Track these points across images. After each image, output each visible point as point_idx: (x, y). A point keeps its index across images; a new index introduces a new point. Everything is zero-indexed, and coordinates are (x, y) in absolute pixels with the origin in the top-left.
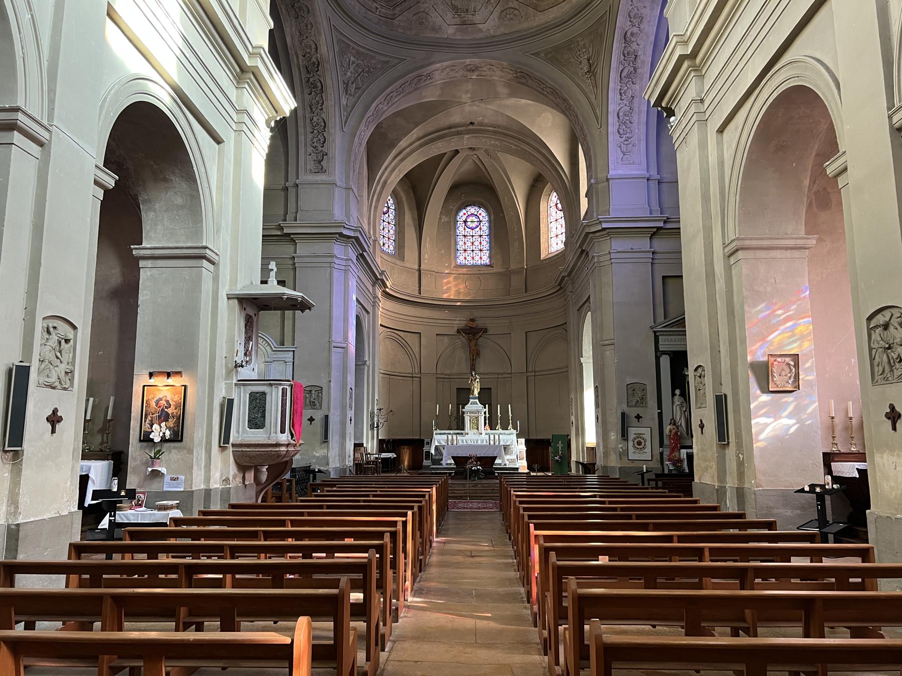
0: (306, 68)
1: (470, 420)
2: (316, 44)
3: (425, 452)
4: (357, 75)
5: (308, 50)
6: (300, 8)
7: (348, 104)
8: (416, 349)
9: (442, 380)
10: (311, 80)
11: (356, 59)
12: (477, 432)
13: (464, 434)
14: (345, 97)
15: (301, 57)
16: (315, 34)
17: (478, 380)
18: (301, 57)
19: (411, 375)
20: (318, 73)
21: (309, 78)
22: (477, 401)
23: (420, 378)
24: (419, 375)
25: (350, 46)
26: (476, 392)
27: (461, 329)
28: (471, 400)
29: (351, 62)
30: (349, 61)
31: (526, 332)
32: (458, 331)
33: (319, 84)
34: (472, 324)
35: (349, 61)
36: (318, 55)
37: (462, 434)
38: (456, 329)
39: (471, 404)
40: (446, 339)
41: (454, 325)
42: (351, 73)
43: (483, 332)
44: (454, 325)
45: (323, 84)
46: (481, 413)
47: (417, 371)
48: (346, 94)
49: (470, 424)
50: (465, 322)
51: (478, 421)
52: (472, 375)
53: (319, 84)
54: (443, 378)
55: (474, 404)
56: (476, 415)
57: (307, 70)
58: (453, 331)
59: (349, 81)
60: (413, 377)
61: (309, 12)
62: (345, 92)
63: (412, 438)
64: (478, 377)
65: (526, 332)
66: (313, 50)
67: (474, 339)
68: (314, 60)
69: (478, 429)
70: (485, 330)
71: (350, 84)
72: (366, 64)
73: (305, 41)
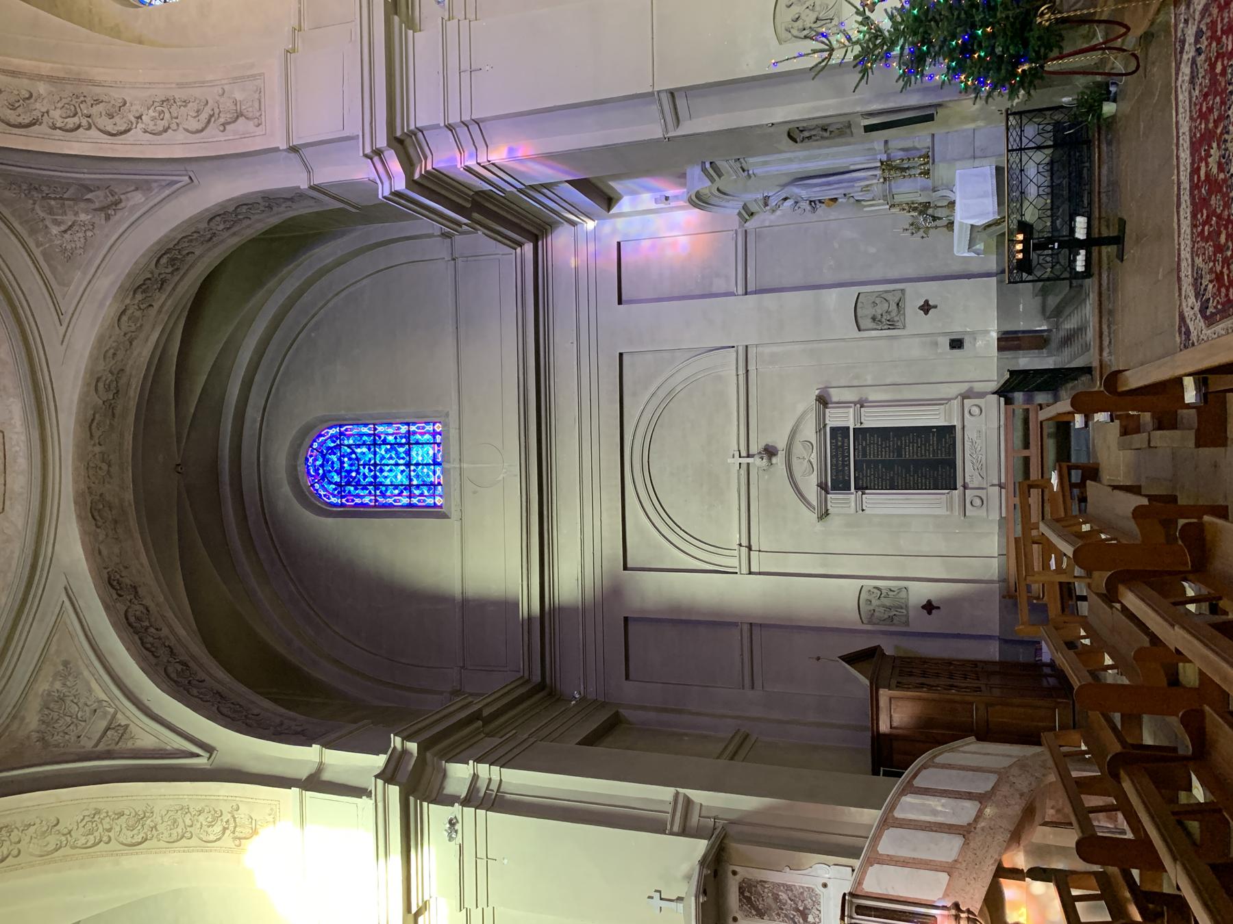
0: (161, 288)
2: (119, 320)
4: (66, 202)
5: (138, 314)
6: (108, 389)
7: (133, 188)
10: (170, 270)
11: (47, 223)
14: (128, 199)
15: (156, 306)
16: (110, 337)
18: (156, 306)
20: (150, 276)
21: (172, 273)
25: (44, 254)
29: (63, 228)
30: (65, 232)
33: (164, 260)
35: (65, 232)
36: (128, 301)
42: (76, 214)
45: (154, 262)
48: (121, 201)
53: (164, 260)
57: (162, 284)
59: (95, 210)
61: (98, 380)
62: (122, 205)
66: (129, 312)
68: (139, 296)
71: (97, 205)
72: (31, 202)
73: (133, 328)
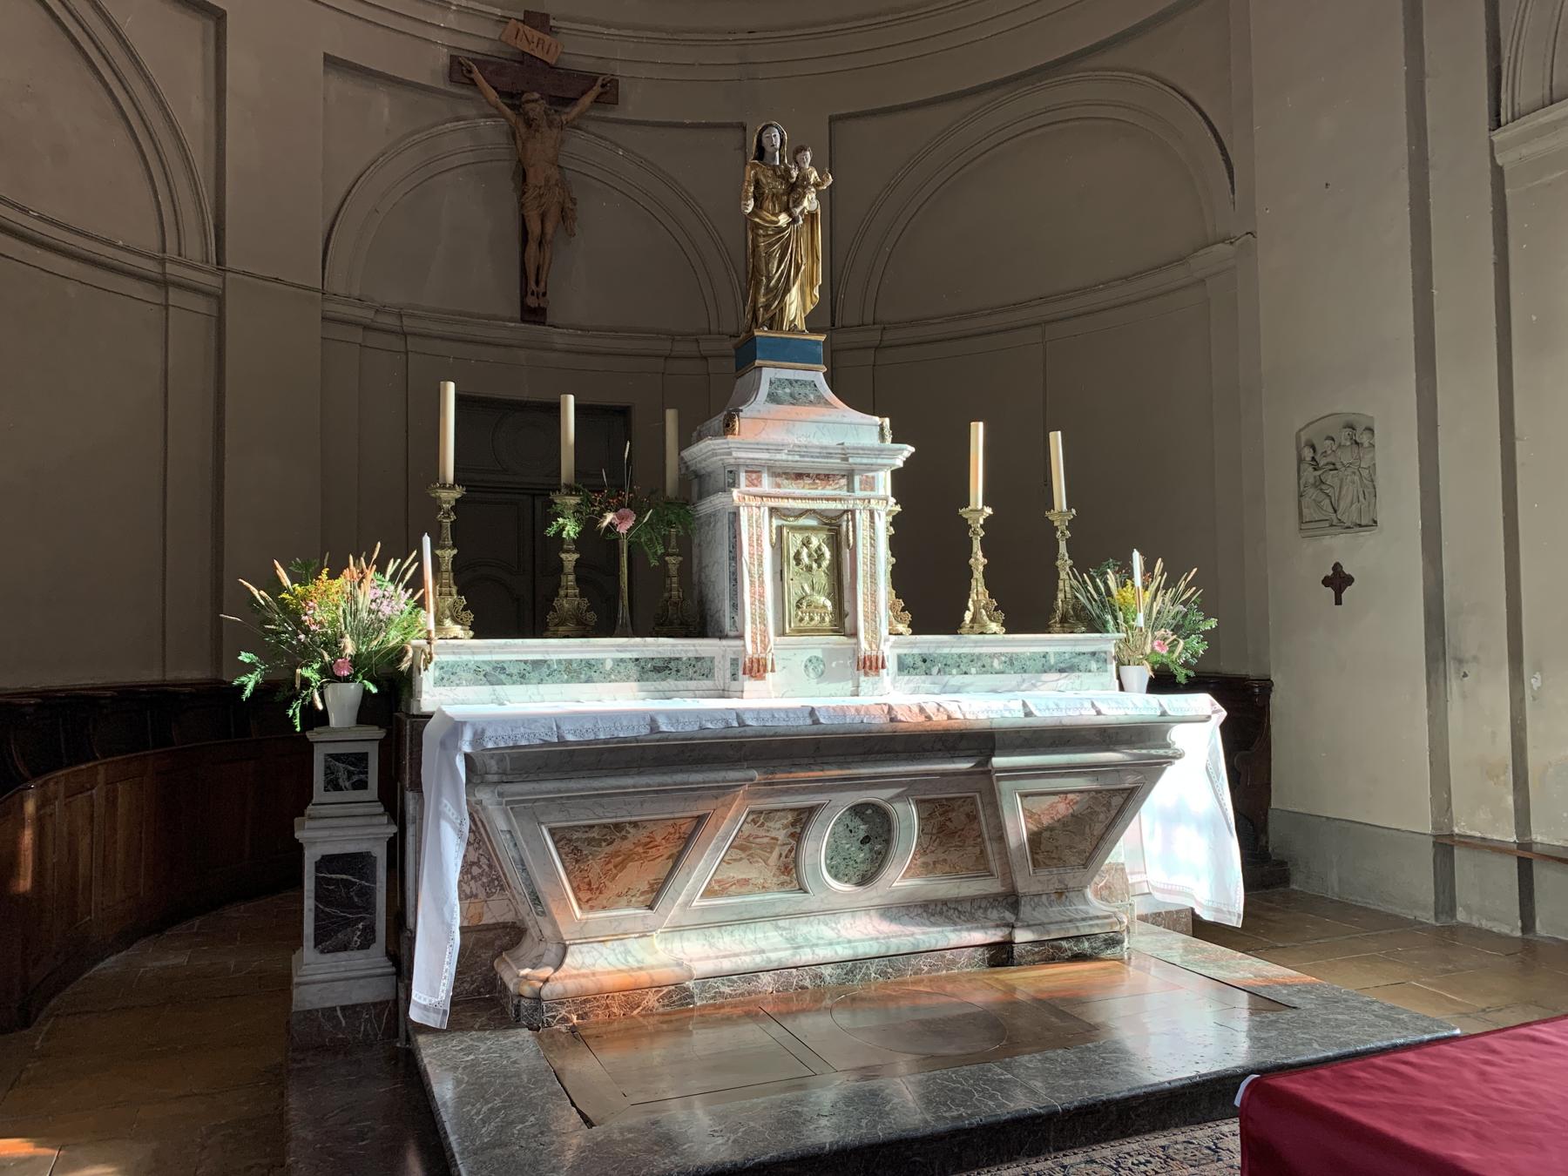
1: (779, 546)
3: (326, 862)
8: (192, 111)
9: (358, 335)
12: (831, 653)
13: (722, 671)
17: (810, 202)
19: (151, 267)
22: (818, 377)
23: (220, 299)
24: (209, 280)
26: (795, 305)
27: (474, 61)
28: (769, 374)
31: (832, 120)
32: (460, 70)
34: (532, 42)
37: (700, 668)
38: (445, 61)
39: (773, 398)
40: (383, 104)
41: (433, 35)
43: (596, 101)
44: (433, 35)
46: (870, 484)
47: (193, 250)
49: (780, 575)
50: (492, 32)
51: (837, 540)
52: (761, 153)
54: (366, 328)
55: (794, 400)
56: (826, 497)
58: (430, 66)
60: (164, 283)
63: (152, 676)
64: (814, 176)
65: (832, 120)
67: (551, 124)
69: (842, 622)
70: (609, 93)
